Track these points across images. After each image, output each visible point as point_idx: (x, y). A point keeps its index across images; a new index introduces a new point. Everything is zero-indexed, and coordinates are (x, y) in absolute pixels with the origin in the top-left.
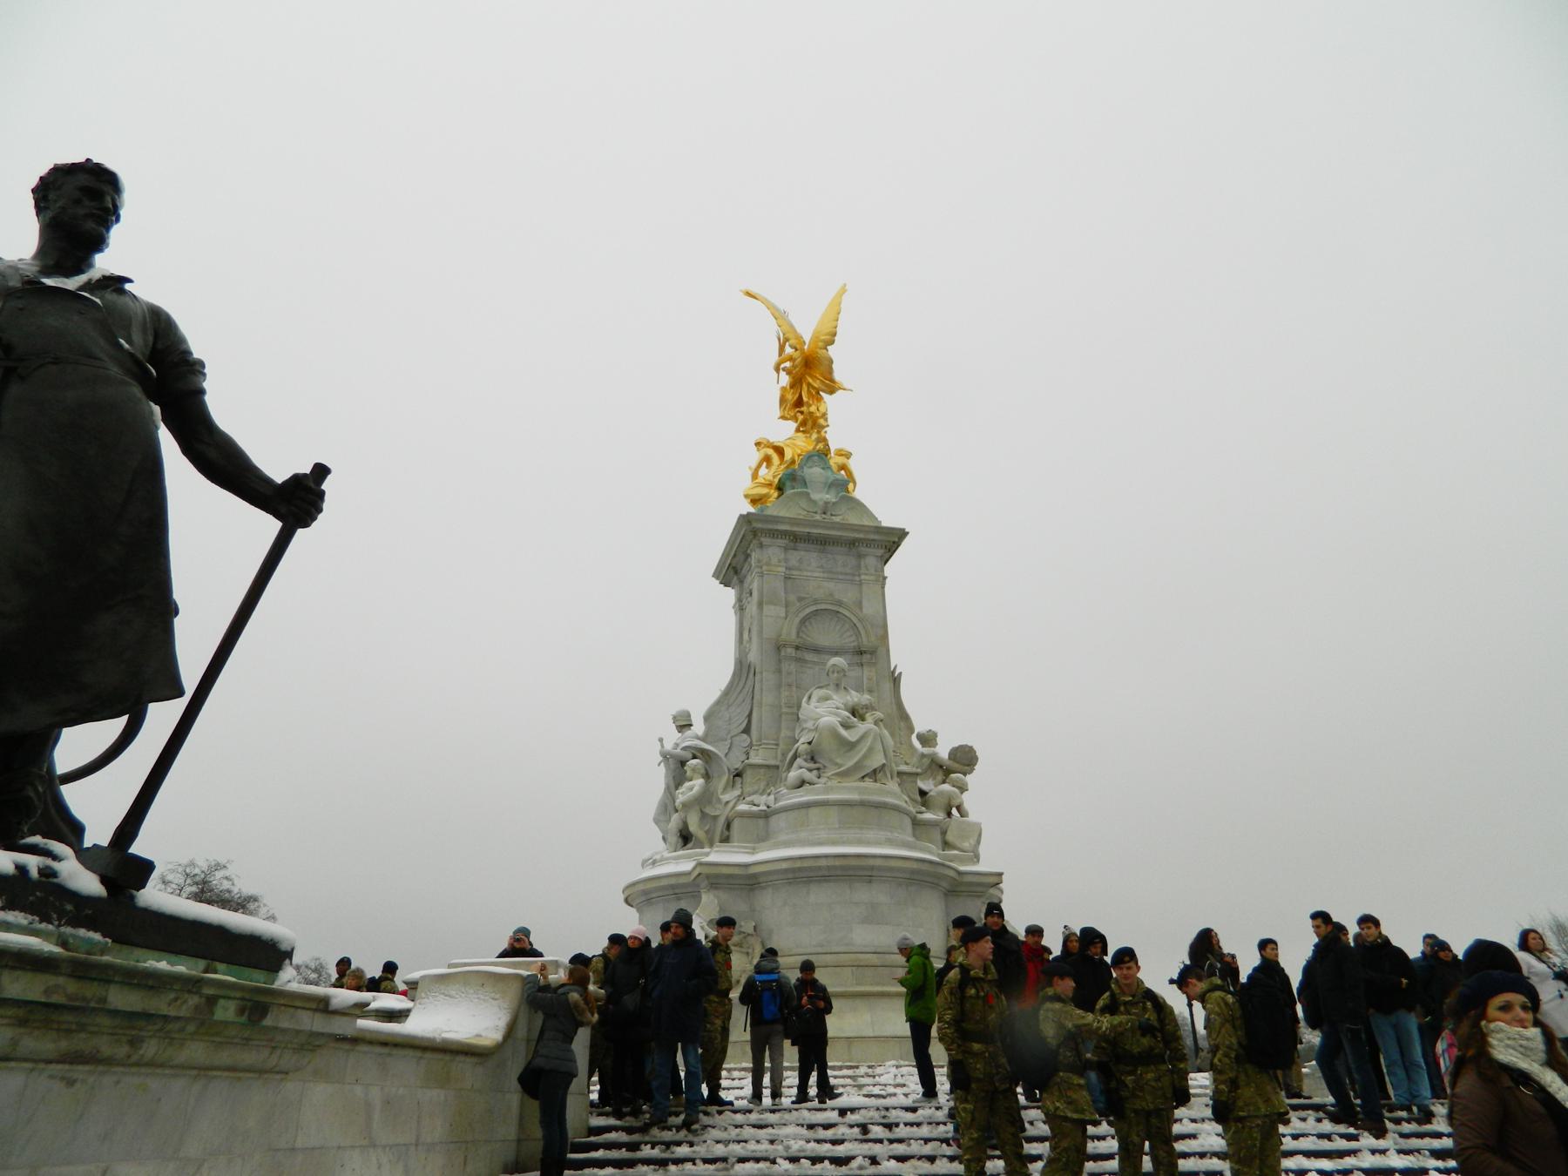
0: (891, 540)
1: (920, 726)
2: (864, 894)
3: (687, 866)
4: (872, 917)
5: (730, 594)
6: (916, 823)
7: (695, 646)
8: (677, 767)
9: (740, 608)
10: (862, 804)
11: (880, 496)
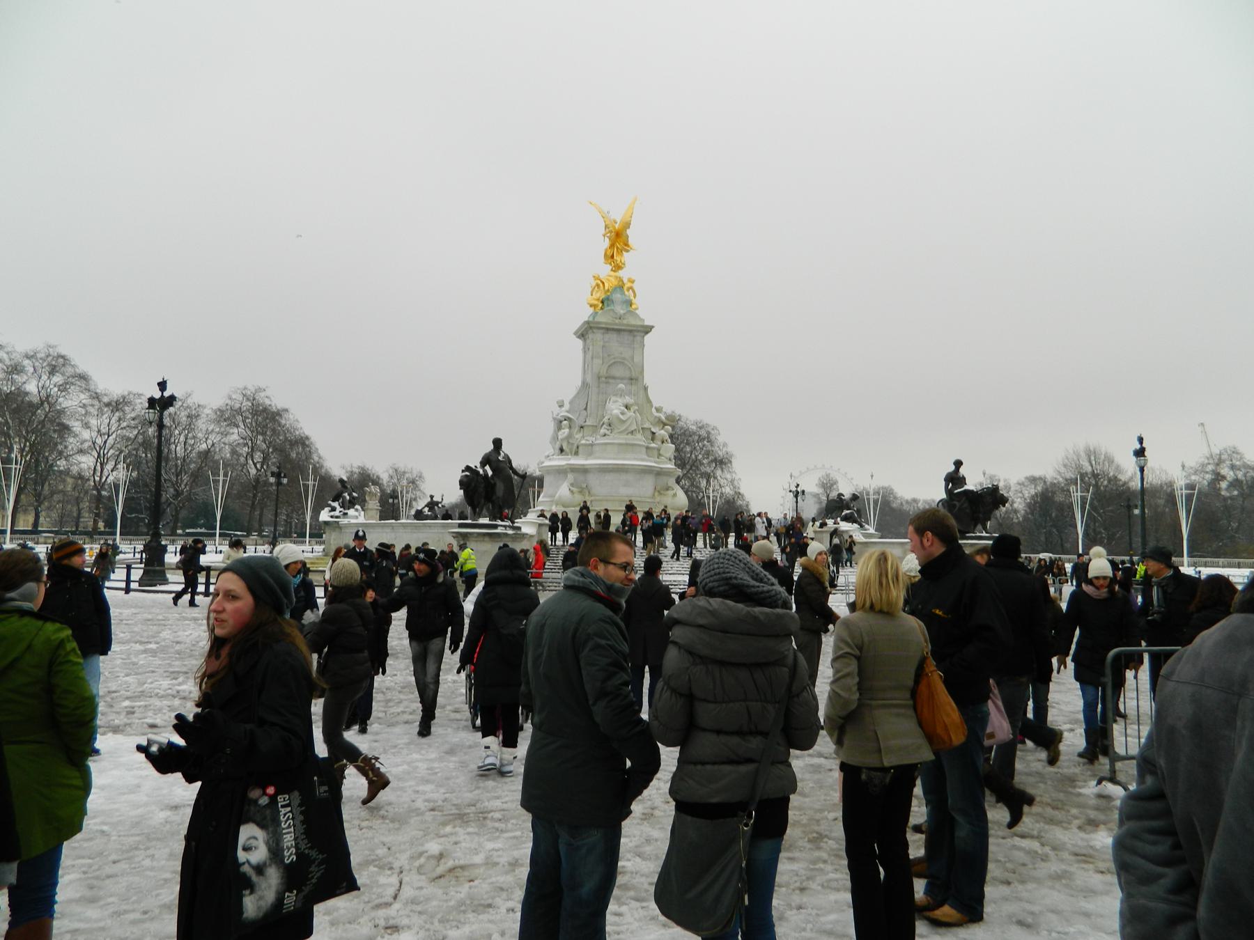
0: (647, 330)
1: (656, 404)
2: (624, 477)
3: (563, 463)
5: (580, 342)
6: (648, 448)
7: (564, 369)
8: (559, 424)
9: (585, 350)
10: (627, 444)
11: (645, 311)
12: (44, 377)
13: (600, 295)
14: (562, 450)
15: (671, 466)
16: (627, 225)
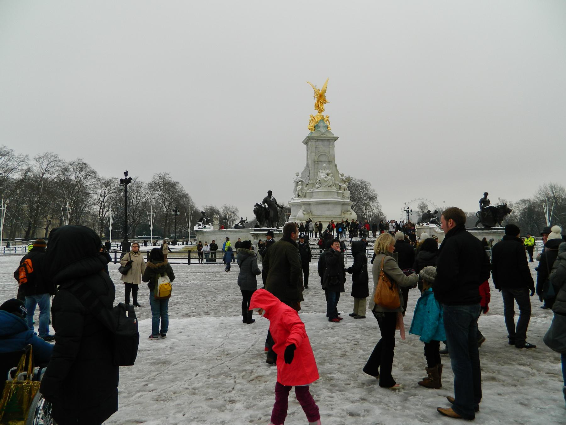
0: (336, 139)
1: (341, 172)
2: (327, 206)
3: (299, 201)
4: (329, 210)
5: (305, 146)
6: (338, 193)
7: (299, 159)
8: (297, 183)
10: (328, 191)
11: (334, 131)
12: (78, 173)
13: (313, 124)
14: (299, 195)
15: (349, 201)
16: (325, 91)
